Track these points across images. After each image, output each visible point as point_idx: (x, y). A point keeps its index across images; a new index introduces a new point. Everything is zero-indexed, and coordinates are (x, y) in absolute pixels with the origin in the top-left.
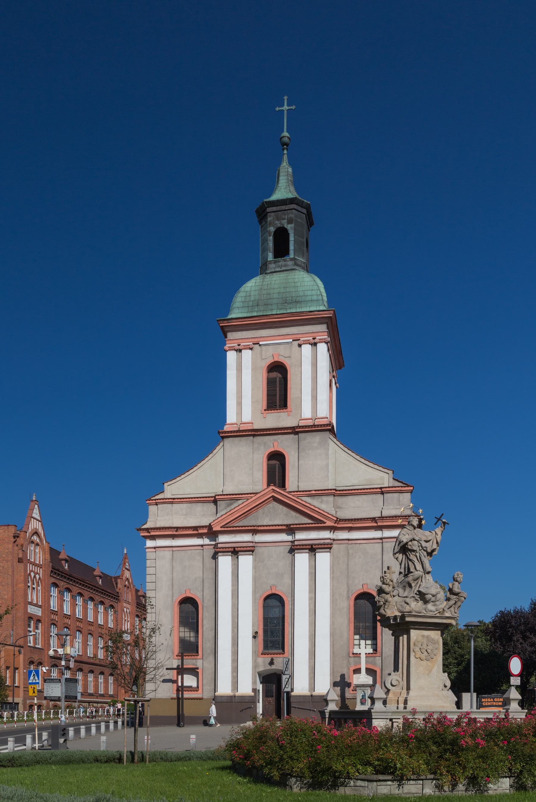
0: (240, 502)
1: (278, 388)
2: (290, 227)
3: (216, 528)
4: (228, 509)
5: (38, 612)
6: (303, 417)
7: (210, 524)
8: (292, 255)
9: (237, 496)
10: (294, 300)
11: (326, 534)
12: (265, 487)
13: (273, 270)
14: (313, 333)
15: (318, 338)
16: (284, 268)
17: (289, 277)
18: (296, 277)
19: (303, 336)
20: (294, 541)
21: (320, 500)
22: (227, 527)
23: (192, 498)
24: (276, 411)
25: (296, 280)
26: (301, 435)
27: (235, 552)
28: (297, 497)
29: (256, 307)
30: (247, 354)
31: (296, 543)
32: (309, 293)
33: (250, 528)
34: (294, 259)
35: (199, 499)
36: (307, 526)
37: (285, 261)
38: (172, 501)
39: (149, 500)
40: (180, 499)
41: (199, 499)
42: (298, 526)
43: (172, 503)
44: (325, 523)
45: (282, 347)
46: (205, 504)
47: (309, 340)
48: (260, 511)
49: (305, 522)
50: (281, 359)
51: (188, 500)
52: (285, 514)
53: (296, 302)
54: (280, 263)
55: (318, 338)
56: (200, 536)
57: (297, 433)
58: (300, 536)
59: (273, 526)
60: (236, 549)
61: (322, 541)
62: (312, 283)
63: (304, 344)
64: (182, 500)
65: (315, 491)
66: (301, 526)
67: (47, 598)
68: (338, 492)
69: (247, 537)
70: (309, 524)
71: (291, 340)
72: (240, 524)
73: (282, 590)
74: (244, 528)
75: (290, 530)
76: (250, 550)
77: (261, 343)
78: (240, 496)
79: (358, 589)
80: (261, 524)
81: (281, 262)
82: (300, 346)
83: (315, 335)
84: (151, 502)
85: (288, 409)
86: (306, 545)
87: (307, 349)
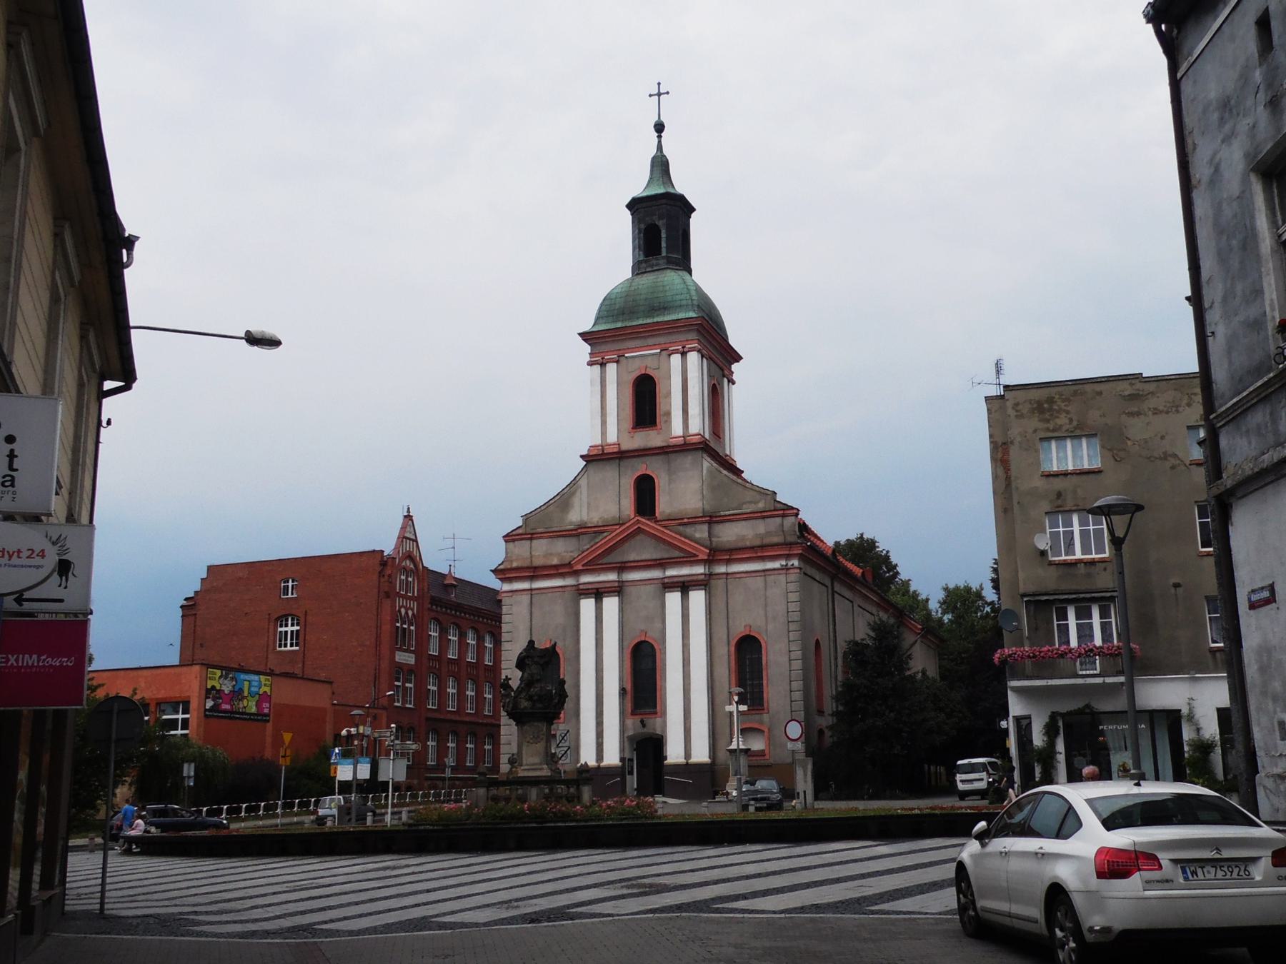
0: (605, 534)
2: (661, 223)
3: (579, 567)
4: (592, 543)
5: (410, 659)
6: (673, 436)
7: (570, 563)
8: (664, 254)
9: (602, 528)
10: (661, 307)
11: (699, 570)
13: (644, 271)
15: (687, 346)
16: (655, 268)
17: (659, 280)
18: (666, 279)
20: (665, 578)
21: (693, 529)
22: (590, 566)
25: (666, 283)
26: (673, 456)
27: (598, 594)
28: (665, 527)
29: (621, 316)
30: (612, 369)
31: (666, 580)
32: (678, 297)
34: (667, 257)
37: (657, 259)
43: (531, 539)
44: (698, 556)
45: (650, 358)
46: (567, 539)
47: (678, 349)
48: (627, 545)
50: (650, 372)
53: (665, 308)
54: (651, 263)
55: (687, 346)
56: (562, 575)
57: (667, 453)
58: (671, 572)
59: (642, 561)
60: (600, 590)
61: (695, 578)
62: (682, 286)
63: (672, 353)
65: (688, 518)
67: (423, 640)
68: (715, 519)
69: (612, 577)
70: (680, 558)
71: (659, 351)
72: (605, 561)
73: (652, 637)
75: (661, 564)
76: (618, 590)
77: (626, 355)
79: (739, 630)
82: (670, 355)
85: (659, 427)
86: (677, 582)
87: (676, 359)
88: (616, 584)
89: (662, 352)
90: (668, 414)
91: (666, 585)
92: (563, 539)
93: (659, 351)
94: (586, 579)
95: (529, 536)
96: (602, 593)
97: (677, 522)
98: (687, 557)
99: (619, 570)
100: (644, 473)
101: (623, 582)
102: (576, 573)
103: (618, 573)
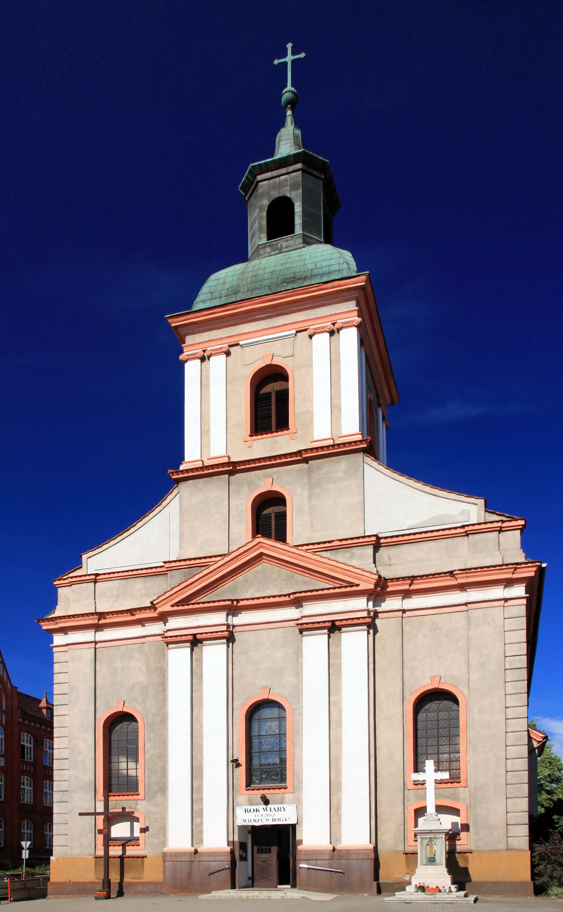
1: (273, 407)
3: (167, 608)
9: (203, 561)
12: (250, 539)
14: (331, 315)
19: (314, 322)
22: (183, 605)
23: (128, 571)
24: (270, 435)
31: (304, 620)
33: (222, 603)
35: (140, 572)
36: (326, 592)
38: (96, 578)
39: (59, 580)
40: (109, 574)
41: (140, 572)
42: (309, 594)
46: (148, 578)
47: (324, 327)
49: (322, 587)
51: (121, 574)
52: (284, 580)
57: (306, 461)
59: (264, 598)
64: (111, 575)
66: (315, 593)
74: (212, 604)
78: (208, 560)
80: (242, 598)
81: (282, 242)
82: (311, 337)
83: (333, 319)
84: (62, 582)
87: (322, 340)
88: (224, 628)
89: (298, 334)
90: (310, 413)
91: (305, 626)
92: (143, 579)
93: (294, 332)
94: (174, 623)
95: (93, 577)
96: (201, 641)
97: (322, 546)
98: (340, 588)
99: (230, 610)
100: (269, 489)
101: (234, 626)
102: (163, 617)
103: (227, 615)
